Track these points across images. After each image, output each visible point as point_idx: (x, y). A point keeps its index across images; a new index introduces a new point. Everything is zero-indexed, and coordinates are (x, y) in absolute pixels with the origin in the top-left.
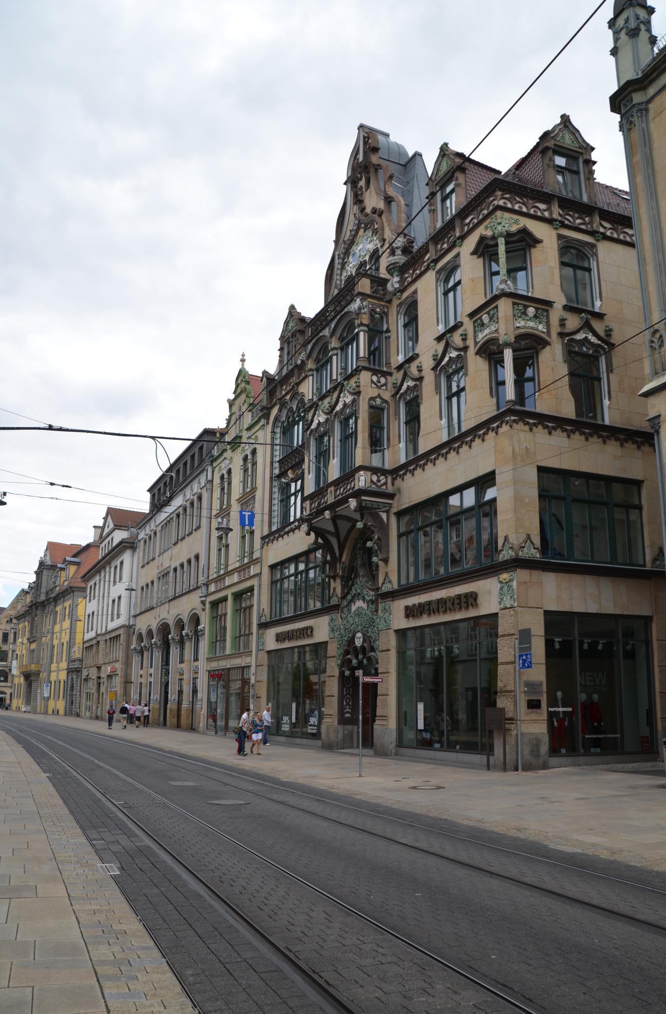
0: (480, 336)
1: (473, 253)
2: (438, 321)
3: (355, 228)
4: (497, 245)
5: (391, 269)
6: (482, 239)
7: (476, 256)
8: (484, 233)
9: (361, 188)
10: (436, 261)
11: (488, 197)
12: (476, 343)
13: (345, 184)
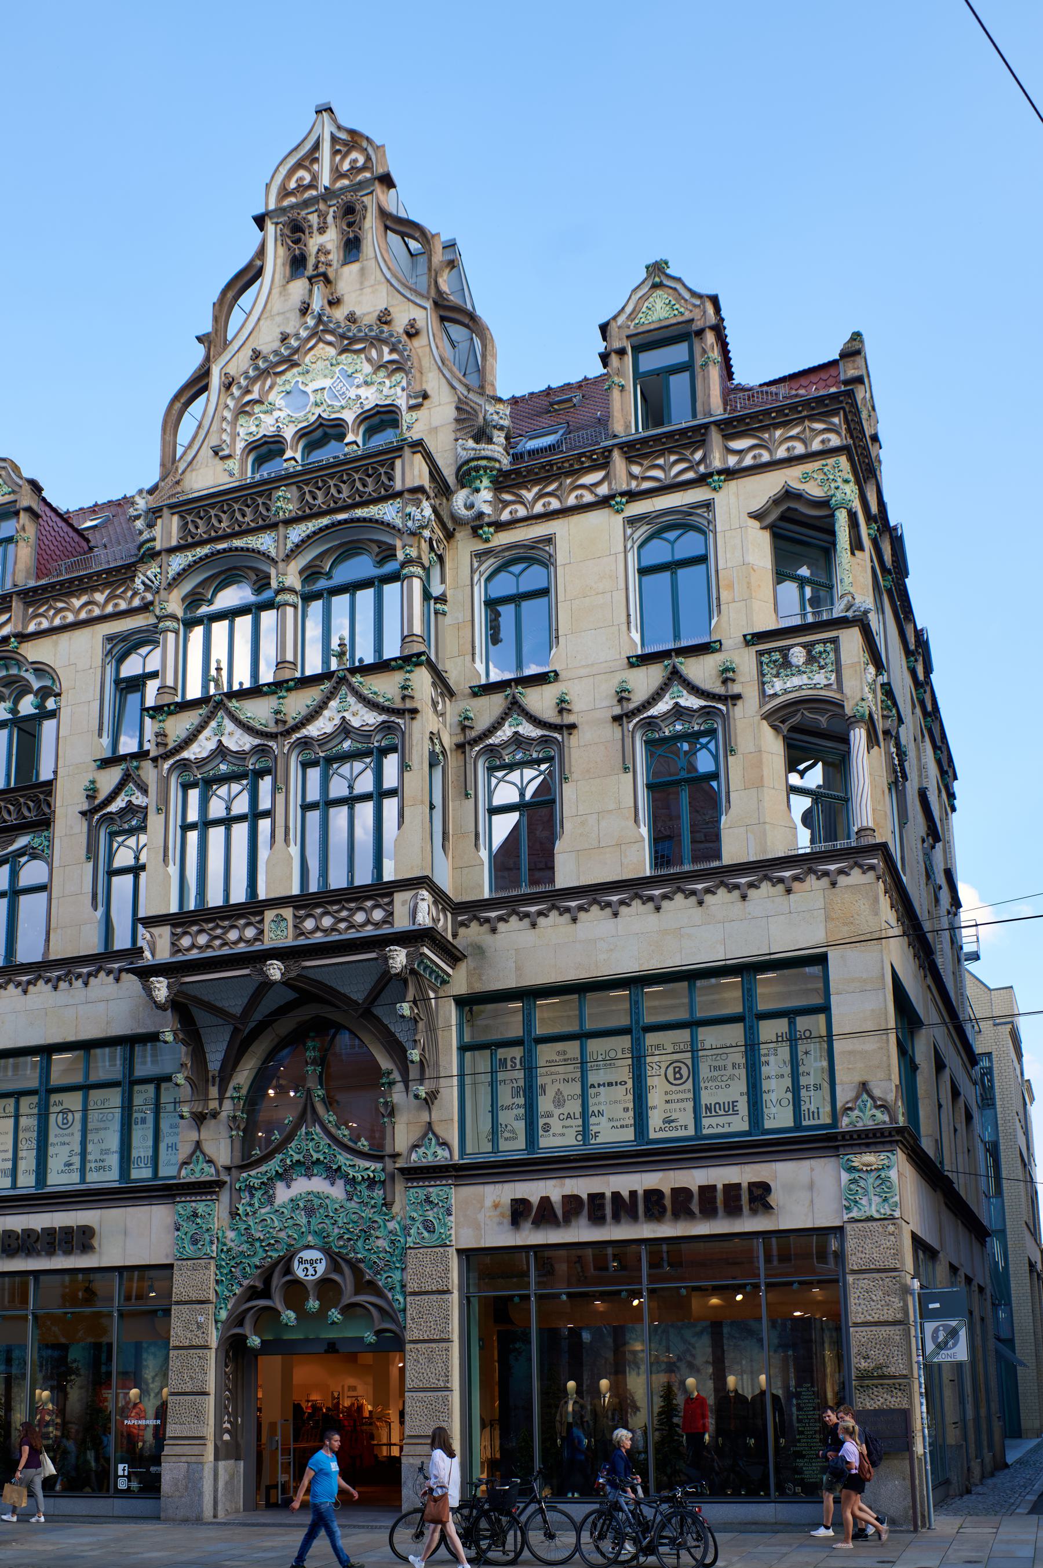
0: (778, 685)
3: (304, 334)
5: (477, 469)
6: (788, 494)
7: (757, 524)
8: (796, 485)
9: (322, 250)
10: (632, 496)
11: (811, 418)
13: (260, 221)
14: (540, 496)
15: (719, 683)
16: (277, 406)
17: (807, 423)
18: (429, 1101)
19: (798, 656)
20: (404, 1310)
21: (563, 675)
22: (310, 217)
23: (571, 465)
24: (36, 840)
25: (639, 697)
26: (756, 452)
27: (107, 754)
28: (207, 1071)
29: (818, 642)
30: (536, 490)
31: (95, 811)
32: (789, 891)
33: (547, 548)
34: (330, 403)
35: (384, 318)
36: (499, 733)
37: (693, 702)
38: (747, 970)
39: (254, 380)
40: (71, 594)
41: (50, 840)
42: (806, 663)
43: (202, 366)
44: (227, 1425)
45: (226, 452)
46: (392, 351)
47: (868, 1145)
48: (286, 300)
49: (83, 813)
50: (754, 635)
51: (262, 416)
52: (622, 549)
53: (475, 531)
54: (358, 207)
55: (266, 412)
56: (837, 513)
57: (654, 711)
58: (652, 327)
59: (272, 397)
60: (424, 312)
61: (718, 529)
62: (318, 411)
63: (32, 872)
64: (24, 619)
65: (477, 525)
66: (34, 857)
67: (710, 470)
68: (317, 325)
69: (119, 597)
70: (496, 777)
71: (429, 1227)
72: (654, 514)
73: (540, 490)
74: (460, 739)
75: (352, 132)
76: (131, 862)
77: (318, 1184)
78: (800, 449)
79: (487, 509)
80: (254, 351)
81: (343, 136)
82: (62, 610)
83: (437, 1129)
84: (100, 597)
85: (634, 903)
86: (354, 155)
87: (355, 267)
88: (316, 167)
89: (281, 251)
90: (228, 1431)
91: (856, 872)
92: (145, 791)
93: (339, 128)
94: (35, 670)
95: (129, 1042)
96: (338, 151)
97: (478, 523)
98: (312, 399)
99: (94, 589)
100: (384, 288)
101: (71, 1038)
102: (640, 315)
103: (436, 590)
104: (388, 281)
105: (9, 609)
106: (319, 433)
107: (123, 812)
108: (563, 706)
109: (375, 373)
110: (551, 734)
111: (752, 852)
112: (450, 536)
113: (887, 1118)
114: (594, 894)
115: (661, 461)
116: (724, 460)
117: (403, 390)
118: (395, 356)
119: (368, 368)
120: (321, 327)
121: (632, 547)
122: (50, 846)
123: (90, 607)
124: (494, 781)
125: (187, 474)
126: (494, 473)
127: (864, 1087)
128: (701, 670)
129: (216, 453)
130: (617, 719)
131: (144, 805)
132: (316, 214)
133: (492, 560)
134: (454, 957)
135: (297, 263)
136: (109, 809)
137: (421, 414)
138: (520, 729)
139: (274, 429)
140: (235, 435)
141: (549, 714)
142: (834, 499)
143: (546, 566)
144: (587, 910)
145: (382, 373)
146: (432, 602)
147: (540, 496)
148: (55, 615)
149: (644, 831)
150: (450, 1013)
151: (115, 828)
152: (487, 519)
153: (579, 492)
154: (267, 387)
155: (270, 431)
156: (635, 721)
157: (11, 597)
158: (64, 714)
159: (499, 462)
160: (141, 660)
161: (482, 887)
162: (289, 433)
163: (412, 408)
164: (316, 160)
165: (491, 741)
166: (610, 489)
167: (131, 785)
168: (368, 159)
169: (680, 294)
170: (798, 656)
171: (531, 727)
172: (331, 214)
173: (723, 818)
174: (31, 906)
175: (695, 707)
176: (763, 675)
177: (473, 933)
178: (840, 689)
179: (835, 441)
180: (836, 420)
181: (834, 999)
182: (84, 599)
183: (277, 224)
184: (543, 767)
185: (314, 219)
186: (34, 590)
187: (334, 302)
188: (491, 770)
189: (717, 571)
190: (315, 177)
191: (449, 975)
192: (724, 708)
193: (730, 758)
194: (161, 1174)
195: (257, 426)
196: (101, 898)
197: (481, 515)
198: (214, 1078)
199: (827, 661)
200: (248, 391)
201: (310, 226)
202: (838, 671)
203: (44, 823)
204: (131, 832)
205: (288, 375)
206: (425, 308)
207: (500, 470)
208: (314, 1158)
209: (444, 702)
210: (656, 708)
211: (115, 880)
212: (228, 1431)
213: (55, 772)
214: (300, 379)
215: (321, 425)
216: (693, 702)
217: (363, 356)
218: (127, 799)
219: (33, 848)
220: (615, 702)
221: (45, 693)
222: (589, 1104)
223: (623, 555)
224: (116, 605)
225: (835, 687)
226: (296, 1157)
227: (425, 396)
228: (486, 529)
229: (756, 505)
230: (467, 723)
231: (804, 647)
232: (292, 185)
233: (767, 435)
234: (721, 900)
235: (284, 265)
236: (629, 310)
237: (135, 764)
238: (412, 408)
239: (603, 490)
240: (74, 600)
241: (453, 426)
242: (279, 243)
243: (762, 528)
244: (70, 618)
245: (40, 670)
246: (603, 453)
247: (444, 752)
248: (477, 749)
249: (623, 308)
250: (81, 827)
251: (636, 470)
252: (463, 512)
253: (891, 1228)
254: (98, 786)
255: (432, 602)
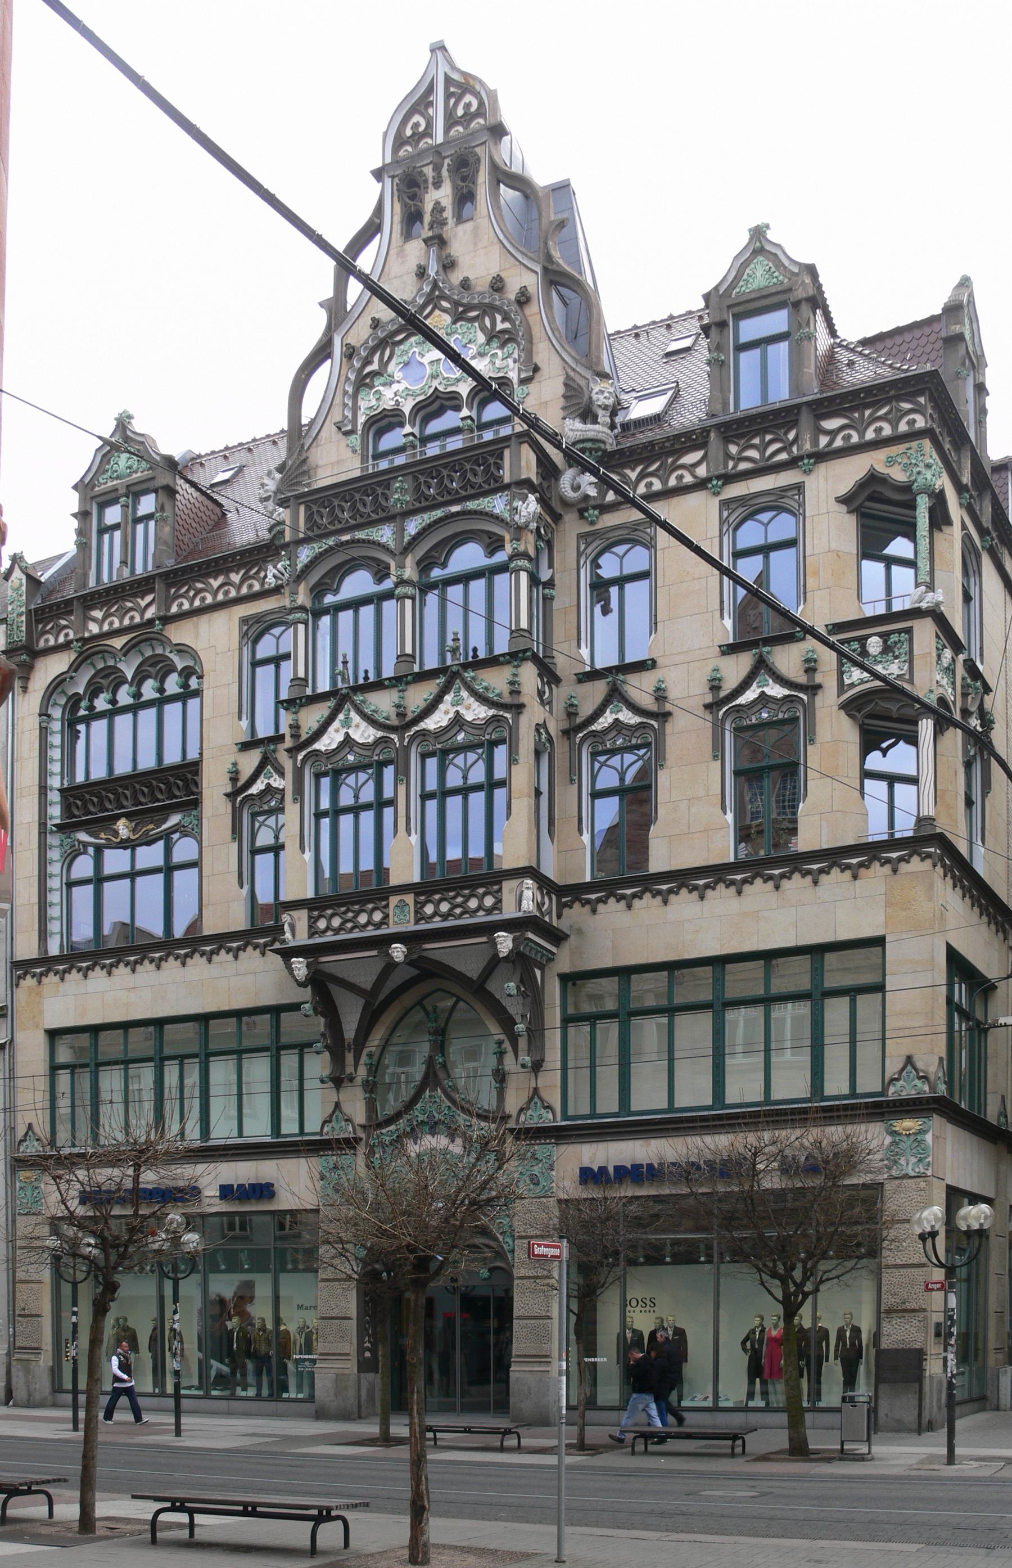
1: (845, 500)
2: (722, 610)
4: (912, 506)
6: (873, 479)
7: (844, 508)
8: (881, 469)
10: (729, 479)
12: (842, 688)
13: (378, 174)
14: (641, 476)
15: (802, 673)
16: (396, 378)
17: (894, 404)
18: (537, 1066)
19: (874, 645)
20: (513, 1251)
21: (659, 661)
22: (425, 170)
23: (673, 445)
24: (186, 819)
25: (730, 684)
26: (846, 432)
27: (246, 738)
28: (343, 1039)
29: (893, 632)
30: (639, 469)
31: (238, 791)
32: (855, 877)
33: (648, 530)
34: (446, 376)
35: (498, 285)
36: (601, 720)
37: (776, 691)
38: (817, 951)
39: (373, 351)
40: (208, 575)
41: (199, 819)
42: (882, 653)
43: (325, 334)
44: (367, 1345)
45: (349, 428)
46: (503, 320)
47: (908, 1112)
48: (403, 262)
49: (227, 795)
50: (835, 625)
51: (381, 388)
52: (718, 534)
53: (581, 512)
54: (471, 160)
55: (384, 385)
56: (919, 498)
57: (742, 700)
58: (753, 296)
59: (392, 367)
60: (534, 276)
61: (807, 514)
62: (435, 383)
63: (184, 849)
64: (166, 600)
65: (583, 507)
66: (185, 835)
67: (801, 453)
68: (433, 290)
69: (252, 577)
70: (599, 762)
71: (535, 1181)
72: (748, 497)
73: (642, 470)
74: (565, 725)
75: (464, 74)
76: (271, 841)
77: (440, 1141)
78: (887, 431)
79: (592, 492)
80: (373, 319)
81: (456, 76)
82: (201, 590)
83: (544, 1094)
84: (235, 578)
85: (718, 887)
86: (468, 98)
87: (468, 226)
88: (430, 111)
89: (398, 207)
90: (368, 1349)
91: (915, 859)
92: (282, 774)
93: (454, 68)
94: (179, 651)
95: (276, 1011)
96: (452, 94)
97: (584, 505)
98: (428, 371)
99: (230, 570)
100: (497, 249)
101: (225, 1007)
102: (741, 283)
103: (545, 575)
104: (501, 241)
105: (152, 590)
106: (436, 406)
107: (263, 794)
108: (660, 695)
109: (488, 344)
110: (649, 721)
111: (824, 839)
112: (557, 518)
113: (926, 1088)
114: (682, 879)
115: (756, 441)
116: (815, 442)
117: (515, 362)
118: (507, 325)
119: (481, 338)
120: (437, 293)
121: (728, 530)
122: (200, 825)
123: (226, 588)
124: (597, 765)
125: (313, 450)
126: (600, 453)
127: (909, 1060)
128: (788, 659)
129: (339, 429)
130: (708, 707)
131: (281, 787)
132: (431, 167)
133: (598, 542)
134: (558, 937)
135: (412, 218)
136: (250, 792)
137: (532, 387)
138: (621, 716)
139: (393, 403)
140: (355, 409)
141: (647, 702)
142: (916, 484)
143: (648, 548)
144: (677, 893)
145: (495, 344)
146: (541, 587)
147: (641, 476)
148: (195, 596)
149: (730, 817)
150: (553, 991)
151: (257, 809)
152: (592, 503)
153: (679, 472)
154: (386, 358)
155: (389, 404)
156: (724, 710)
157: (154, 579)
158: (207, 694)
159: (604, 442)
160: (275, 640)
161: (584, 870)
162: (407, 410)
163: (523, 382)
164: (431, 104)
165: (593, 728)
166: (708, 471)
167: (269, 767)
168: (481, 104)
169: (780, 261)
170: (874, 645)
171: (630, 714)
172: (445, 167)
173: (801, 805)
174: (184, 881)
175: (779, 696)
176: (843, 665)
177: (576, 915)
178: (911, 681)
179: (920, 422)
180: (922, 400)
181: (888, 979)
182: (221, 579)
183: (393, 177)
184: (642, 752)
185: (429, 171)
186: (175, 572)
187: (448, 265)
188: (594, 755)
189: (804, 557)
190: (429, 124)
191: (553, 954)
192: (805, 698)
193: (809, 747)
194: (306, 1131)
195: (377, 399)
196: (246, 876)
197: (586, 497)
198: (349, 1046)
199: (901, 651)
200: (368, 362)
201: (426, 181)
202: (911, 662)
203: (195, 804)
204: (271, 812)
205: (407, 344)
206: (536, 273)
207: (605, 451)
208: (436, 1119)
209: (551, 690)
210: (744, 696)
211: (258, 858)
212: (368, 1349)
213: (201, 754)
214: (417, 350)
215: (438, 397)
216: (776, 691)
217: (476, 324)
218: (266, 781)
219: (184, 826)
220: (708, 691)
221: (187, 673)
222: (674, 1070)
223: (718, 539)
224: (250, 586)
225: (907, 677)
226: (421, 1118)
227: (536, 369)
228: (591, 512)
229: (845, 487)
230: (571, 710)
231: (880, 637)
232: (409, 132)
233: (856, 415)
234: (796, 885)
235: (402, 222)
236: (730, 279)
237: (272, 747)
238: (523, 382)
239: (702, 471)
240: (211, 581)
241: (561, 402)
242: (396, 198)
243: (849, 512)
244: (209, 600)
245: (182, 650)
246: (702, 432)
247: (550, 740)
248: (581, 735)
249: (725, 277)
250: (225, 808)
251: (733, 449)
252: (570, 494)
253: (923, 1185)
254: (240, 768)
255: (541, 587)
